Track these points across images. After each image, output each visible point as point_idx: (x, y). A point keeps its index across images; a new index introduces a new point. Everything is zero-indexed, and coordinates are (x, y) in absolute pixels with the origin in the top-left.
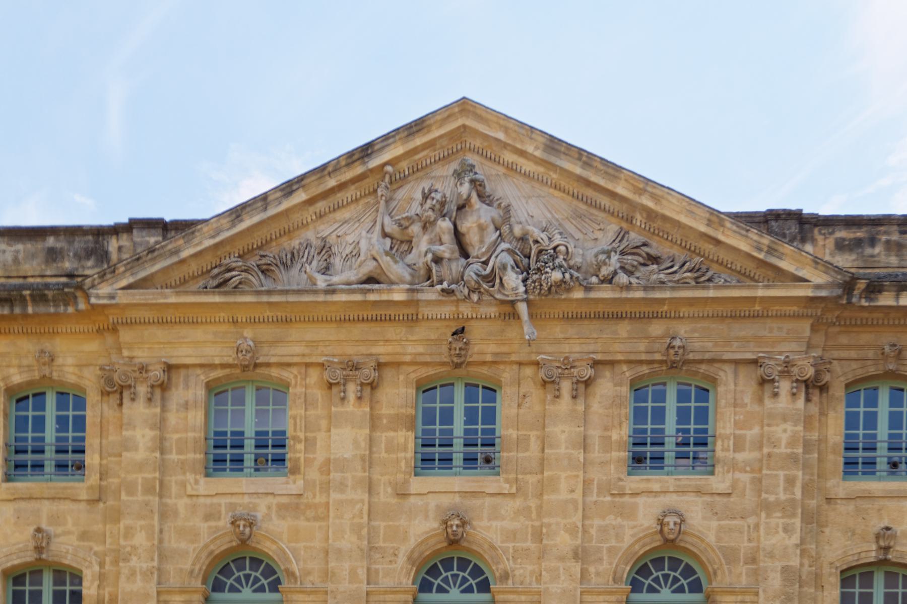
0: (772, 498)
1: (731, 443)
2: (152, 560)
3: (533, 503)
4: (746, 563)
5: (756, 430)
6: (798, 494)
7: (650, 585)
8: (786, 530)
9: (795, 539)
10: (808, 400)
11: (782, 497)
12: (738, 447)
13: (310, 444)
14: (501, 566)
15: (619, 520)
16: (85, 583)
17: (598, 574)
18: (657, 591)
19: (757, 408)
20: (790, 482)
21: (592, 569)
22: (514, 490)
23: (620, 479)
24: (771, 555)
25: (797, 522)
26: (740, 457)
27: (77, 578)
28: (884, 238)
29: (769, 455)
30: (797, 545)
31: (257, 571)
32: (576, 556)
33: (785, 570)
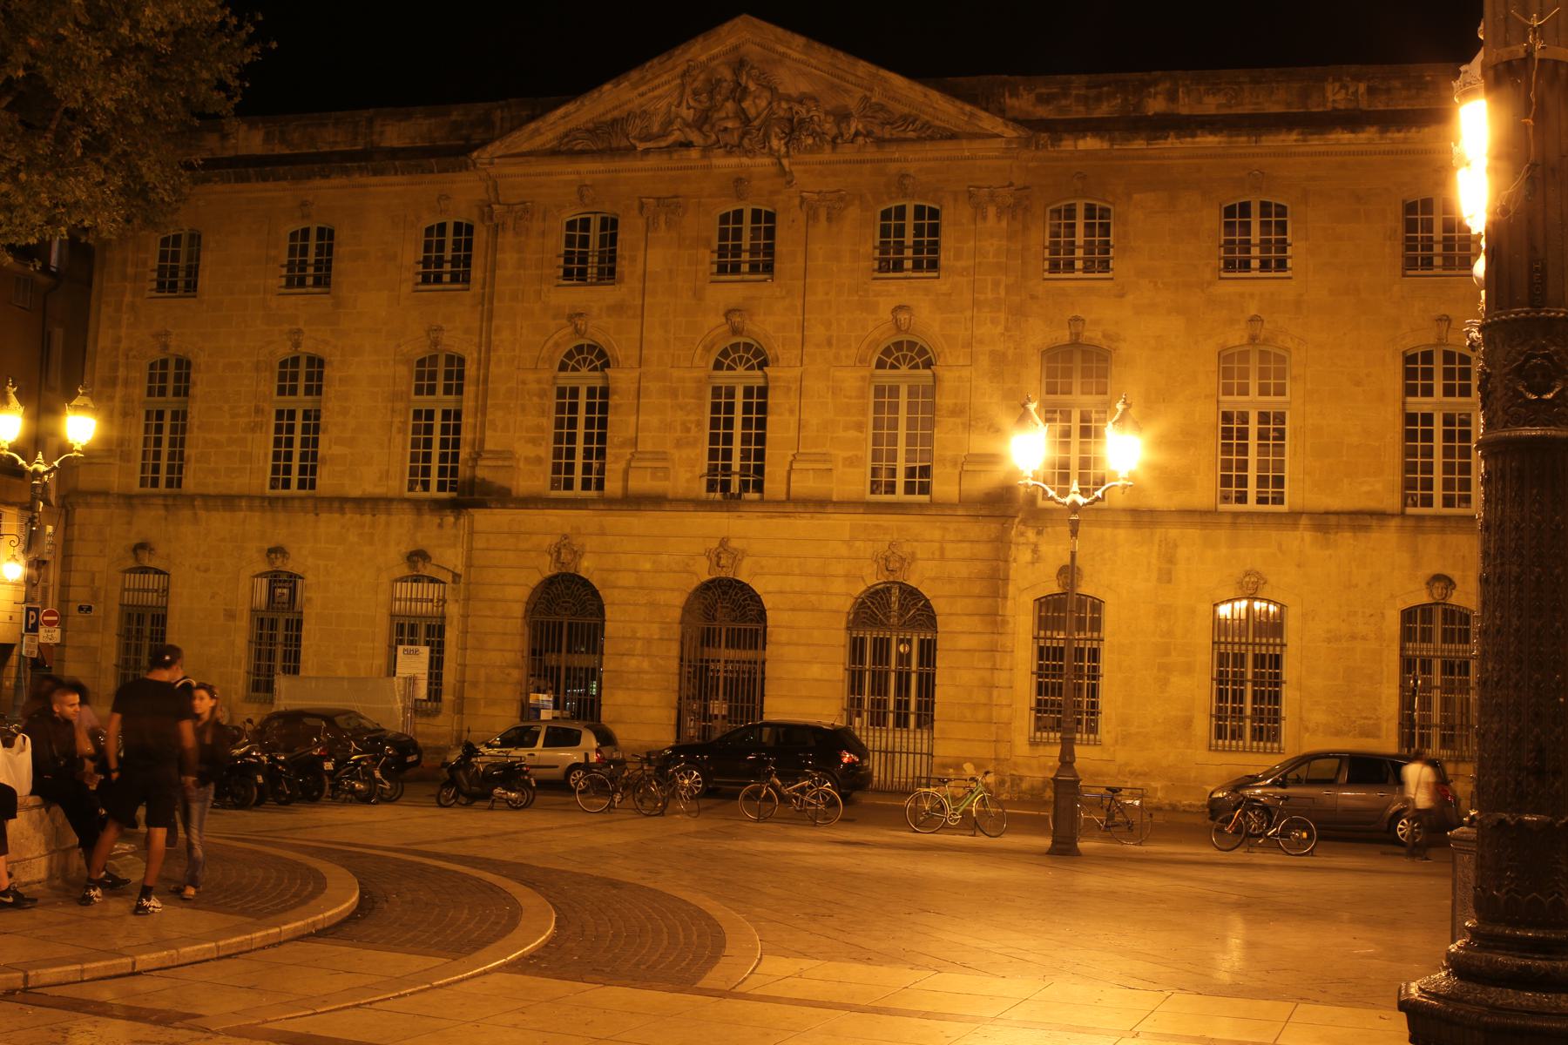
0: (982, 297)
1: (952, 254)
2: (514, 350)
3: (799, 303)
4: (963, 347)
5: (972, 243)
6: (1002, 292)
7: (892, 363)
8: (993, 321)
9: (1000, 329)
10: (1014, 218)
11: (990, 296)
12: (958, 256)
13: (633, 260)
14: (773, 351)
15: (864, 315)
16: (467, 366)
17: (847, 357)
18: (897, 368)
19: (973, 227)
20: (996, 284)
21: (843, 353)
22: (784, 293)
23: (865, 283)
24: (981, 342)
25: (1002, 316)
26: (960, 264)
27: (462, 361)
28: (1074, 92)
29: (980, 263)
30: (1003, 334)
31: (592, 355)
32: (829, 344)
33: (992, 353)
